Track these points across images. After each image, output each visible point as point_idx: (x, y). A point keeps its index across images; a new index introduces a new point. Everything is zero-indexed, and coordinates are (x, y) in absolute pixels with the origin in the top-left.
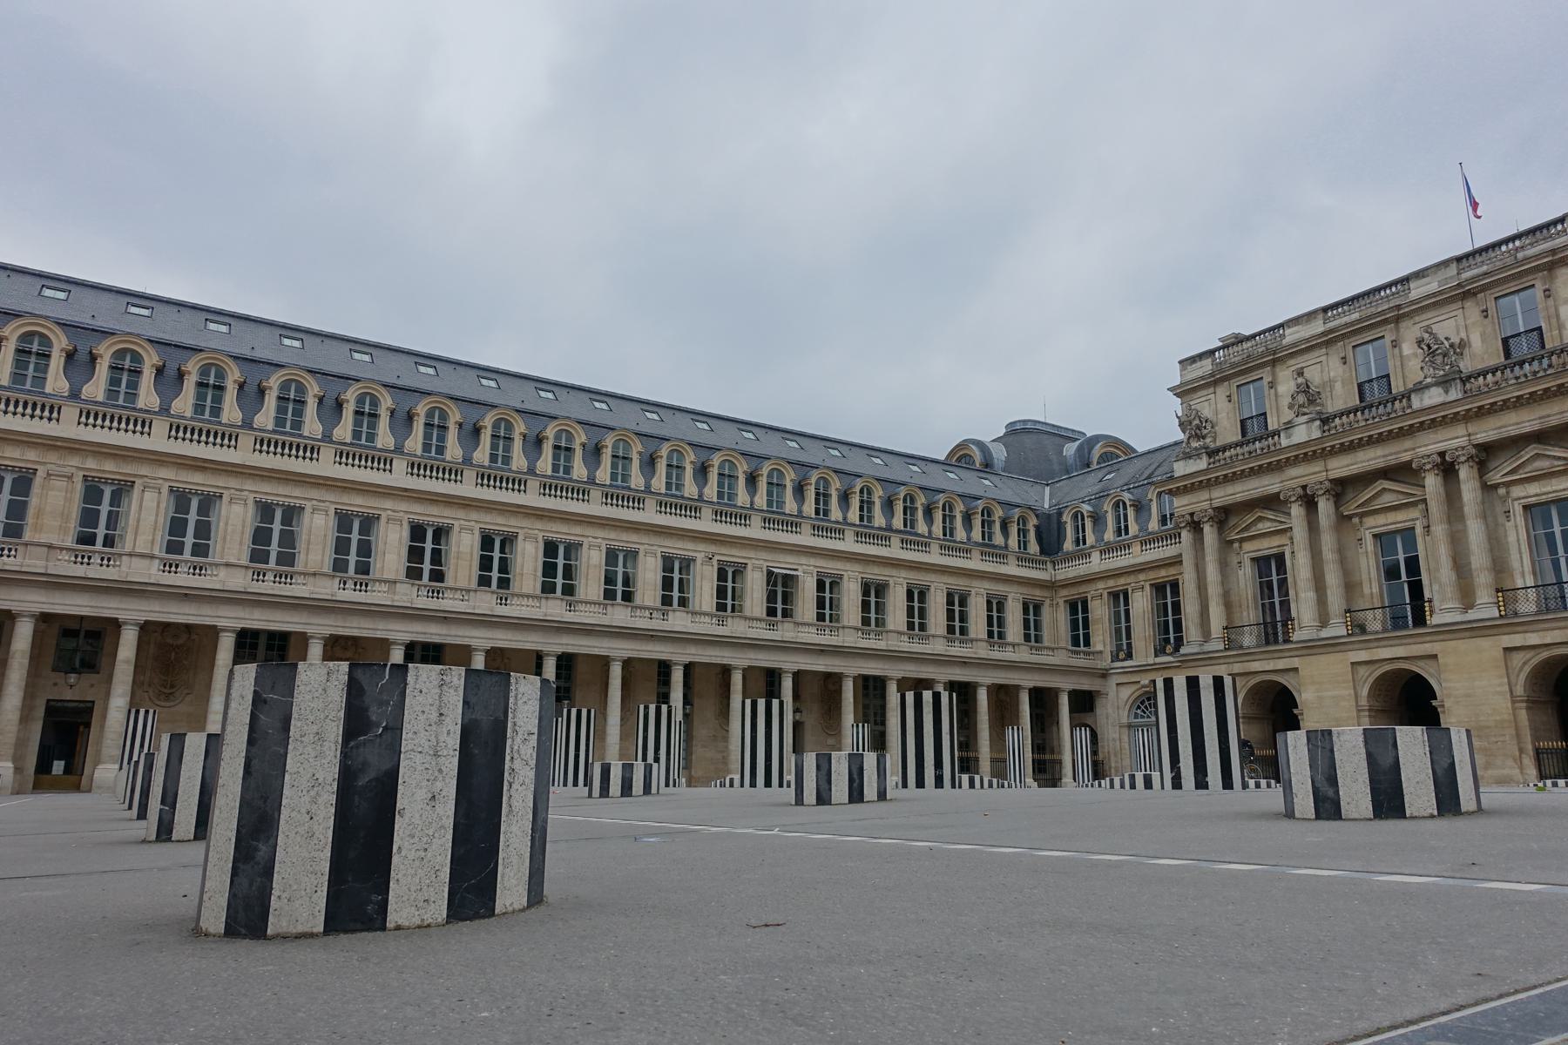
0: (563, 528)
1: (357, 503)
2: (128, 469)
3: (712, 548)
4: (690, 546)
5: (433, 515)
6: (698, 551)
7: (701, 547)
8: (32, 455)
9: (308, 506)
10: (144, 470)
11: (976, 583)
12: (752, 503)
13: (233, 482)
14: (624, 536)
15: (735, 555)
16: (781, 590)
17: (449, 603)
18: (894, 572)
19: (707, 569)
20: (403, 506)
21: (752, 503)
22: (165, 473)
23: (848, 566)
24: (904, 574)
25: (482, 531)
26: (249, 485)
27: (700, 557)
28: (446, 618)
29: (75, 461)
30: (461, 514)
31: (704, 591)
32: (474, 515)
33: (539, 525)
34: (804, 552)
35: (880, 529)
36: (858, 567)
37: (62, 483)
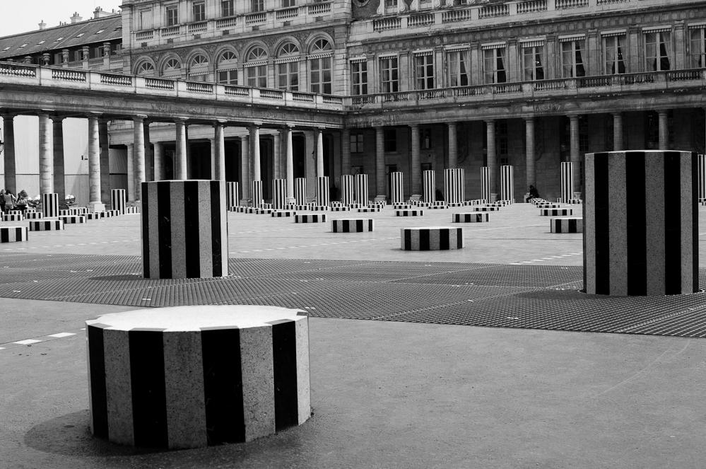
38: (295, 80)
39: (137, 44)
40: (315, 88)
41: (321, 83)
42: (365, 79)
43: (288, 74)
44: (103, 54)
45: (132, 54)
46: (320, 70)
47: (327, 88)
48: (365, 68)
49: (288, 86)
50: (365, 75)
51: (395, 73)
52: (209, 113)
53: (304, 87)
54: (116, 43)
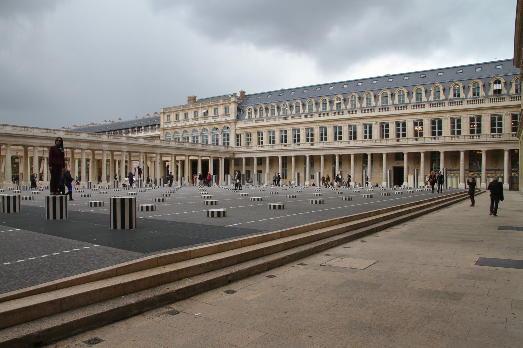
0: (337, 123)
1: (296, 127)
2: (262, 129)
3: (378, 120)
4: (371, 120)
5: (309, 126)
6: (372, 121)
7: (375, 120)
8: (250, 130)
9: (288, 129)
10: (264, 129)
11: (484, 112)
12: (393, 103)
13: (276, 128)
14: (352, 121)
15: (384, 120)
16: (401, 128)
17: (301, 147)
18: (444, 115)
19: (376, 126)
20: (304, 125)
21: (393, 103)
22: (267, 128)
23: (425, 116)
24: (448, 114)
25: (320, 128)
26: (278, 127)
27: (374, 123)
28: (300, 150)
29: (255, 129)
30: (315, 124)
31: (376, 132)
32: (318, 124)
33: (332, 123)
34: (409, 115)
35: (442, 100)
36: (429, 116)
37: (254, 134)
38: (217, 140)
39: (166, 126)
40: (224, 144)
41: (226, 141)
42: (241, 141)
43: (215, 138)
44: (156, 128)
45: (164, 129)
46: (226, 137)
47: (228, 144)
48: (241, 137)
49: (215, 142)
50: (241, 139)
51: (251, 139)
52: (183, 152)
53: (221, 143)
54: (159, 125)
